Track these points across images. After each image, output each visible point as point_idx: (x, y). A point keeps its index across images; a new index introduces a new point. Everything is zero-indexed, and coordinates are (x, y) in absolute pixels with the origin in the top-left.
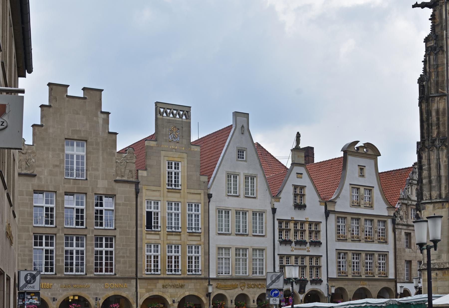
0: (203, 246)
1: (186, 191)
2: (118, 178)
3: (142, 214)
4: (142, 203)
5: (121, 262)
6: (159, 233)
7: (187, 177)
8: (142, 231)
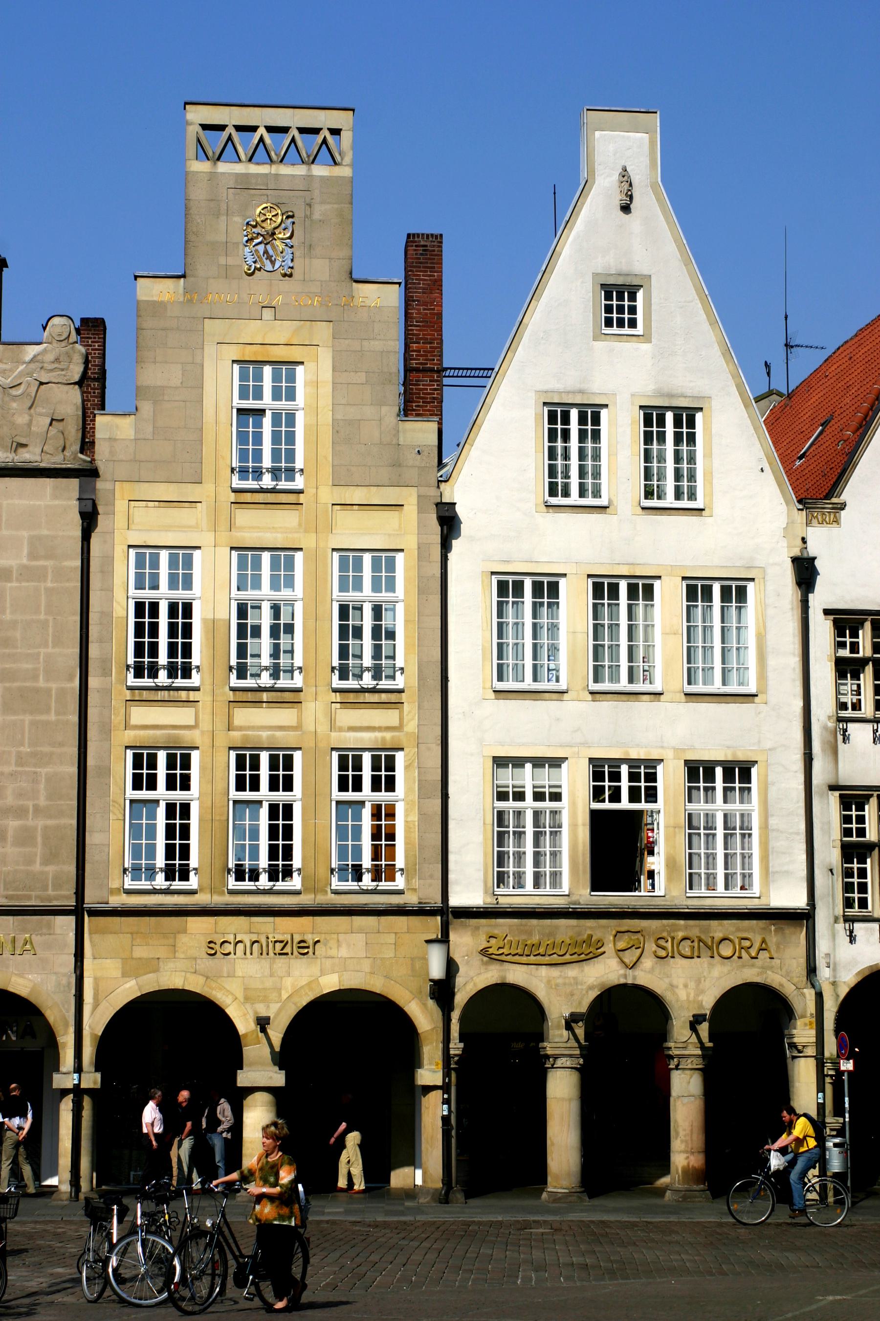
1: (327, 495)
3: (107, 615)
4: (109, 560)
5: (10, 834)
6: (193, 696)
7: (336, 432)
8: (107, 692)
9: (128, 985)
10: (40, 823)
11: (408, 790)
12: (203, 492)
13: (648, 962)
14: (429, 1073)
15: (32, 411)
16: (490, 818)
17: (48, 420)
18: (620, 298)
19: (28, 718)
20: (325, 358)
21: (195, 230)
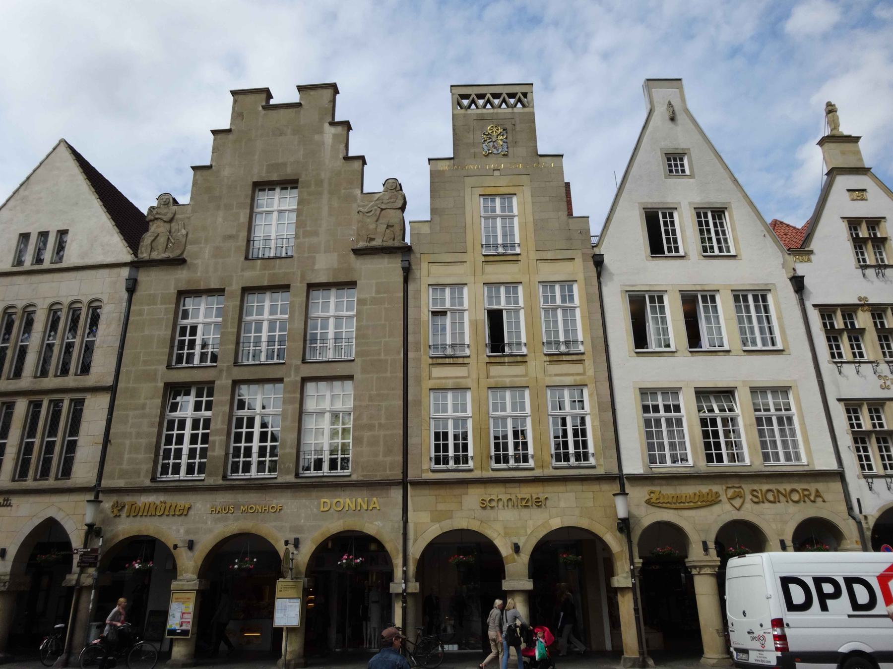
0: (592, 386)
1: (533, 256)
2: (362, 244)
3: (418, 320)
4: (419, 292)
5: (365, 439)
6: (466, 360)
7: (535, 224)
8: (419, 360)
9: (434, 527)
10: (382, 433)
11: (592, 407)
12: (468, 257)
13: (748, 505)
14: (622, 578)
16: (642, 423)
18: (675, 160)
19: (375, 376)
20: (527, 192)
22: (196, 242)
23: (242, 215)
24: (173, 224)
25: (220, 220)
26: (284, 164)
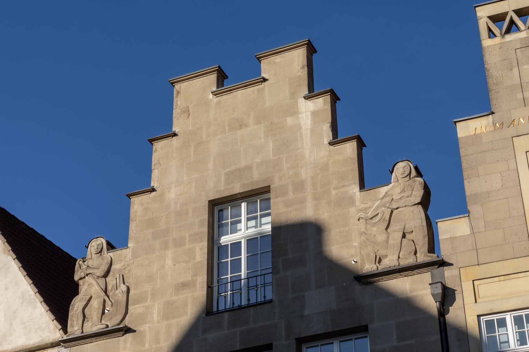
15: (388, 230)
17: (401, 234)
21: (495, 82)
22: (141, 299)
23: (197, 249)
24: (108, 279)
25: (169, 262)
26: (249, 168)
